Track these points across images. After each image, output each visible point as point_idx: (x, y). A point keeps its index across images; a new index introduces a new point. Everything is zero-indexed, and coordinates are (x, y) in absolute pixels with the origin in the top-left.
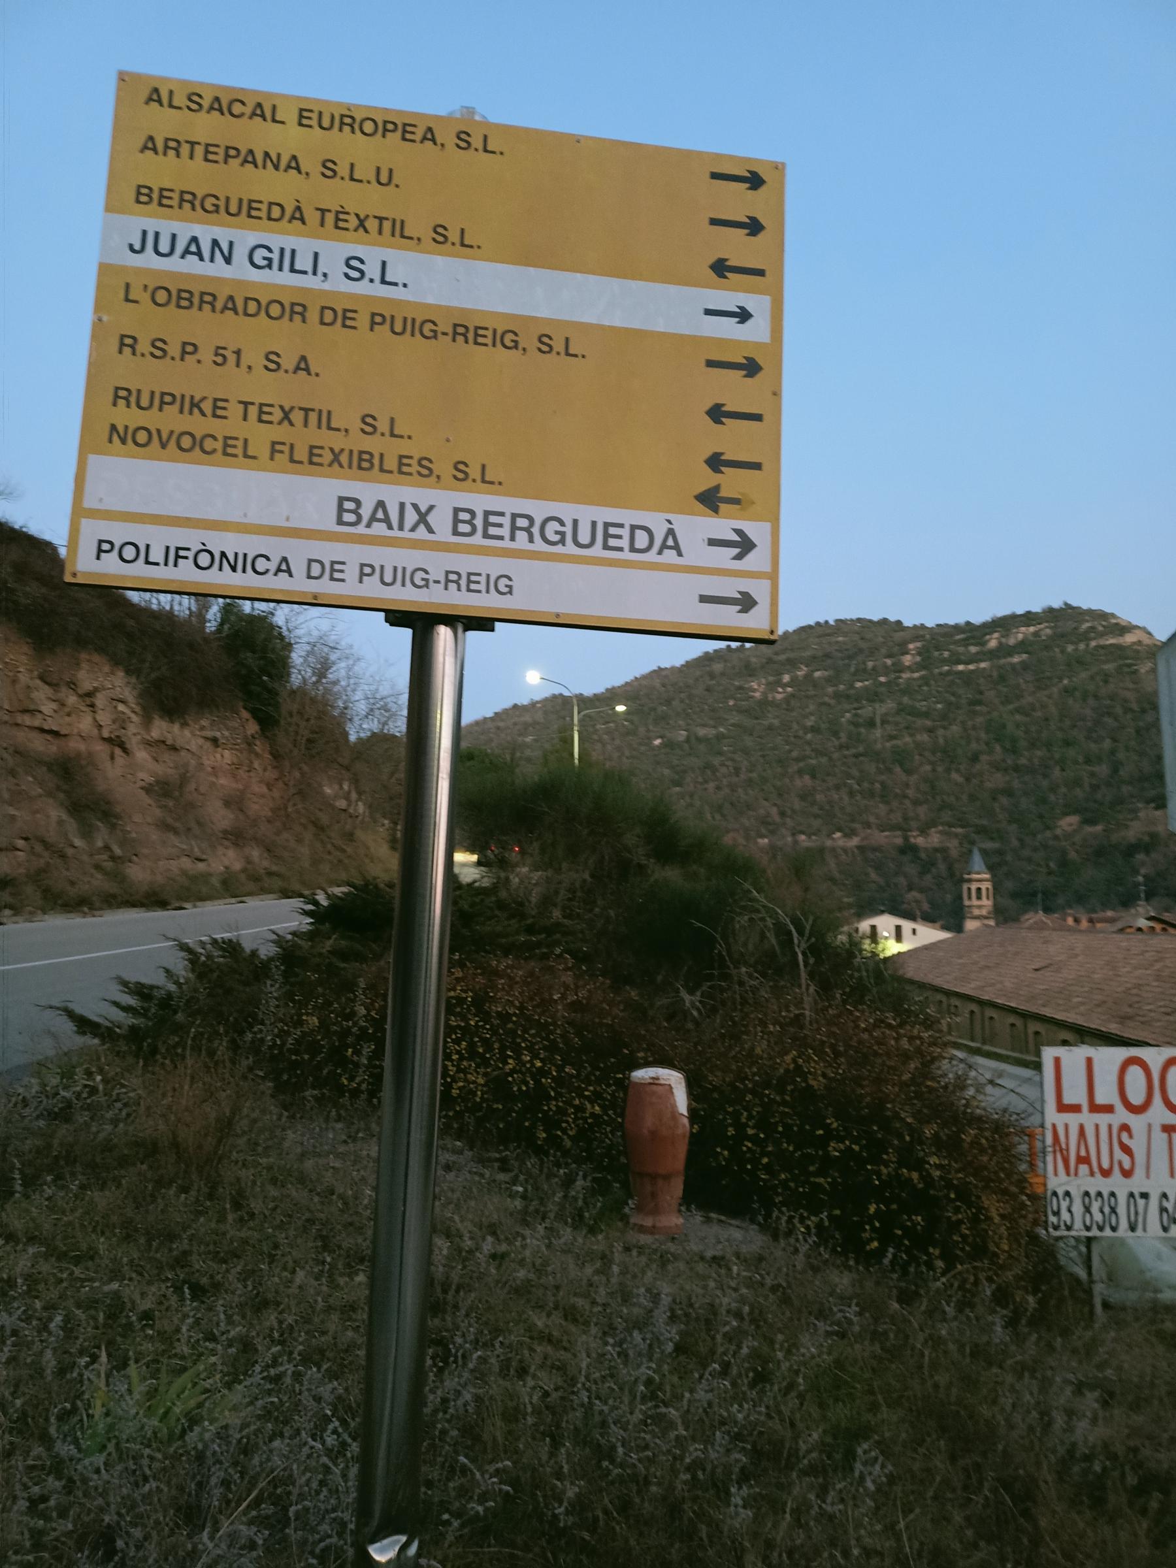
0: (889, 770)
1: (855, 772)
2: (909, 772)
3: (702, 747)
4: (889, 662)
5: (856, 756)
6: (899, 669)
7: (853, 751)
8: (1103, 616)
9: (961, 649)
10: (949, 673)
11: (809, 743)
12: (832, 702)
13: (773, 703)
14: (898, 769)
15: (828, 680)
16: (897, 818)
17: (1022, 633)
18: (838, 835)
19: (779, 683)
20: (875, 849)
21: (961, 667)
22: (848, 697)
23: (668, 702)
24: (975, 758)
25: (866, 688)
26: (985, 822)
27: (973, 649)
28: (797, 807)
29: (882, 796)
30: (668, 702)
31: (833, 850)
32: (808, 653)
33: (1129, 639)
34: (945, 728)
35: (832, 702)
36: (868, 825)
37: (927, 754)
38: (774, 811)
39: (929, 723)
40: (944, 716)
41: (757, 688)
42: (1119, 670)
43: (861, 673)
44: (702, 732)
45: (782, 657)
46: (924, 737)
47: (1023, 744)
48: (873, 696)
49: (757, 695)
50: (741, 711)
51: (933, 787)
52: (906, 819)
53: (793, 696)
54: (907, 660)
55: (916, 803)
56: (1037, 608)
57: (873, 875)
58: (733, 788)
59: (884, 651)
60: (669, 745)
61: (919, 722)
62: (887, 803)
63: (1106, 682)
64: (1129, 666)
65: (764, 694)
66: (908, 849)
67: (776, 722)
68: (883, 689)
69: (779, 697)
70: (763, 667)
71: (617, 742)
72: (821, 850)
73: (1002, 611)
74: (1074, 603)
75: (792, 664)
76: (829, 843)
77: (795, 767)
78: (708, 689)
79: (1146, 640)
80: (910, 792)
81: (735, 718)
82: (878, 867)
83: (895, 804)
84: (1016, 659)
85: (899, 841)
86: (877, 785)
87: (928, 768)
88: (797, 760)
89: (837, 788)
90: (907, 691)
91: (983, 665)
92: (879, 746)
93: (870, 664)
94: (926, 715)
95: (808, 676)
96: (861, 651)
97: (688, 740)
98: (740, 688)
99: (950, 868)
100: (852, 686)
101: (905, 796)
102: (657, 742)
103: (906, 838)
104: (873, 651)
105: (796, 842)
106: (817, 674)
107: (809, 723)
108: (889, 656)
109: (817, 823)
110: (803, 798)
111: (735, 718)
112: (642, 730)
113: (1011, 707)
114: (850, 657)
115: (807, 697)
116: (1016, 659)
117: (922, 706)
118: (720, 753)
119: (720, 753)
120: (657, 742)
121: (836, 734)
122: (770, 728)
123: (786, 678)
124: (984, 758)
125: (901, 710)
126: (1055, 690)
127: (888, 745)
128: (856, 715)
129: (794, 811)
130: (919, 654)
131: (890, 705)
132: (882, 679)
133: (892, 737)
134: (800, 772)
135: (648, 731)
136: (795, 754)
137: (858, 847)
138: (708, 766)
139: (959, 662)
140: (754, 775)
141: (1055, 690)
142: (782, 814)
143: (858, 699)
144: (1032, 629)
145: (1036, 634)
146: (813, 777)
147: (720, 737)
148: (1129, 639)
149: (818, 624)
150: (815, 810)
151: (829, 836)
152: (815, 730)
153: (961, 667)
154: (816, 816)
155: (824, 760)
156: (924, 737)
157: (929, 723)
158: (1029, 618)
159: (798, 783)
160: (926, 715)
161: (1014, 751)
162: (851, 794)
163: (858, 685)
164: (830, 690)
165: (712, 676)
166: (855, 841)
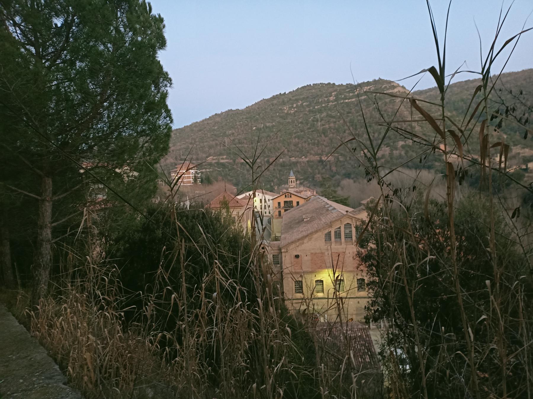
0: (321, 136)
1: (311, 137)
2: (326, 136)
3: (267, 130)
4: (326, 99)
5: (312, 131)
6: (328, 101)
7: (312, 130)
8: (390, 82)
9: (348, 94)
10: (343, 103)
11: (299, 127)
12: (308, 113)
13: (290, 114)
14: (323, 136)
15: (308, 106)
16: (320, 152)
17: (366, 89)
18: (303, 157)
19: (292, 107)
20: (311, 162)
21: (347, 101)
22: (313, 111)
23: (259, 115)
24: (345, 132)
25: (318, 109)
26: (343, 152)
27: (351, 94)
28: (293, 149)
29: (317, 144)
30: (259, 115)
31: (300, 162)
32: (301, 97)
33: (396, 90)
34: (339, 121)
35: (308, 113)
36: (311, 154)
37: (332, 130)
38: (286, 150)
39: (334, 120)
40: (339, 118)
41: (286, 108)
42: (390, 102)
43: (318, 103)
44: (268, 124)
45: (294, 98)
46: (332, 125)
47: (358, 126)
48: (320, 111)
49: (286, 111)
50: (281, 117)
51: (332, 141)
52: (322, 151)
53: (296, 111)
54: (331, 98)
55: (326, 146)
56: (371, 80)
57: (310, 170)
58: (275, 143)
59: (325, 95)
60: (259, 129)
61: (332, 120)
62: (318, 147)
63: (386, 105)
64: (393, 100)
65: (288, 111)
66: (321, 161)
67: (290, 120)
68: (323, 109)
69: (292, 112)
70: (288, 102)
71: (242, 128)
72: (297, 162)
73: (360, 82)
74: (382, 78)
75: (297, 100)
76: (301, 160)
77: (294, 136)
78: (271, 110)
79: (402, 90)
80: (325, 143)
81: (278, 119)
82: (312, 167)
83: (320, 147)
84: (363, 98)
85: (319, 159)
86: (316, 141)
87: (332, 135)
88: (295, 133)
89: (305, 142)
90: (330, 109)
91: (353, 100)
92: (319, 128)
93: (320, 100)
94: (333, 117)
95: (302, 104)
96: (318, 95)
97: (263, 128)
98: (280, 109)
99: (330, 167)
100: (314, 108)
101: (323, 144)
102: (254, 128)
103: (321, 158)
104: (322, 96)
105: (290, 160)
106: (304, 104)
107: (300, 121)
108: (326, 97)
109: (297, 154)
110: (295, 145)
111: (278, 119)
112: (250, 124)
113: (358, 114)
114: (314, 98)
115: (301, 111)
116: (363, 98)
117: (333, 114)
118: (273, 132)
119: (273, 132)
120: (254, 128)
121: (307, 124)
122: (289, 123)
123: (295, 105)
124: (347, 132)
125: (328, 116)
126: (371, 108)
127: (322, 127)
128: (314, 118)
129: (292, 150)
130: (335, 96)
131: (324, 114)
132: (323, 105)
133: (323, 125)
134: (295, 137)
135: (252, 124)
136: (295, 131)
137: (307, 161)
138: (269, 136)
139: (346, 99)
140: (281, 139)
141: (371, 108)
142: (288, 151)
143: (315, 112)
144: (368, 87)
145: (370, 89)
146: (299, 139)
147: (273, 126)
148: (396, 90)
149: (308, 85)
150: (298, 149)
151: (301, 158)
152: (301, 123)
153: (347, 101)
154: (298, 151)
155: (302, 133)
156: (332, 125)
157: (334, 120)
158: (368, 83)
159: (294, 141)
160: (333, 117)
161: (356, 129)
162: (309, 144)
163: (316, 107)
164: (307, 109)
165: (273, 105)
166: (307, 160)
